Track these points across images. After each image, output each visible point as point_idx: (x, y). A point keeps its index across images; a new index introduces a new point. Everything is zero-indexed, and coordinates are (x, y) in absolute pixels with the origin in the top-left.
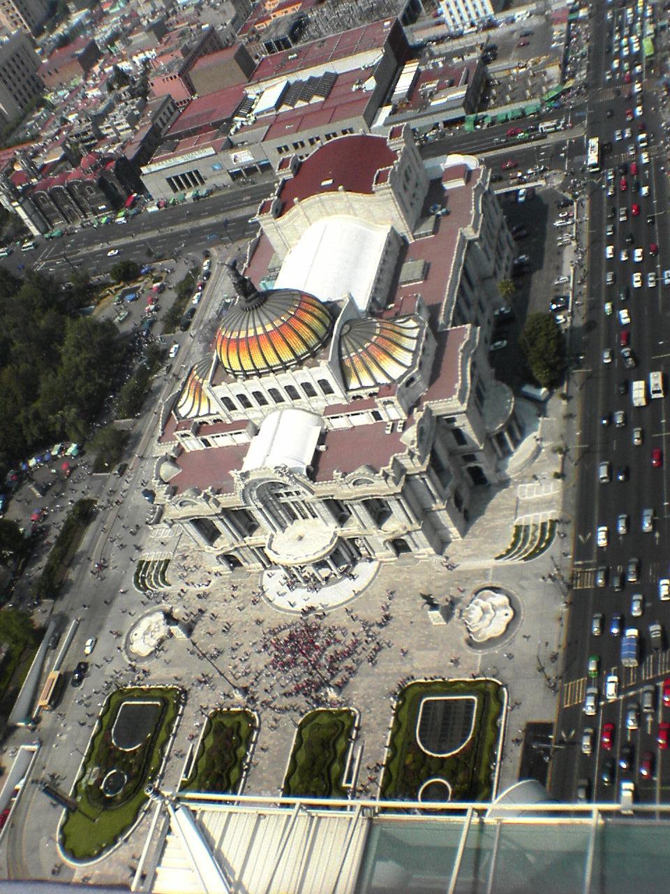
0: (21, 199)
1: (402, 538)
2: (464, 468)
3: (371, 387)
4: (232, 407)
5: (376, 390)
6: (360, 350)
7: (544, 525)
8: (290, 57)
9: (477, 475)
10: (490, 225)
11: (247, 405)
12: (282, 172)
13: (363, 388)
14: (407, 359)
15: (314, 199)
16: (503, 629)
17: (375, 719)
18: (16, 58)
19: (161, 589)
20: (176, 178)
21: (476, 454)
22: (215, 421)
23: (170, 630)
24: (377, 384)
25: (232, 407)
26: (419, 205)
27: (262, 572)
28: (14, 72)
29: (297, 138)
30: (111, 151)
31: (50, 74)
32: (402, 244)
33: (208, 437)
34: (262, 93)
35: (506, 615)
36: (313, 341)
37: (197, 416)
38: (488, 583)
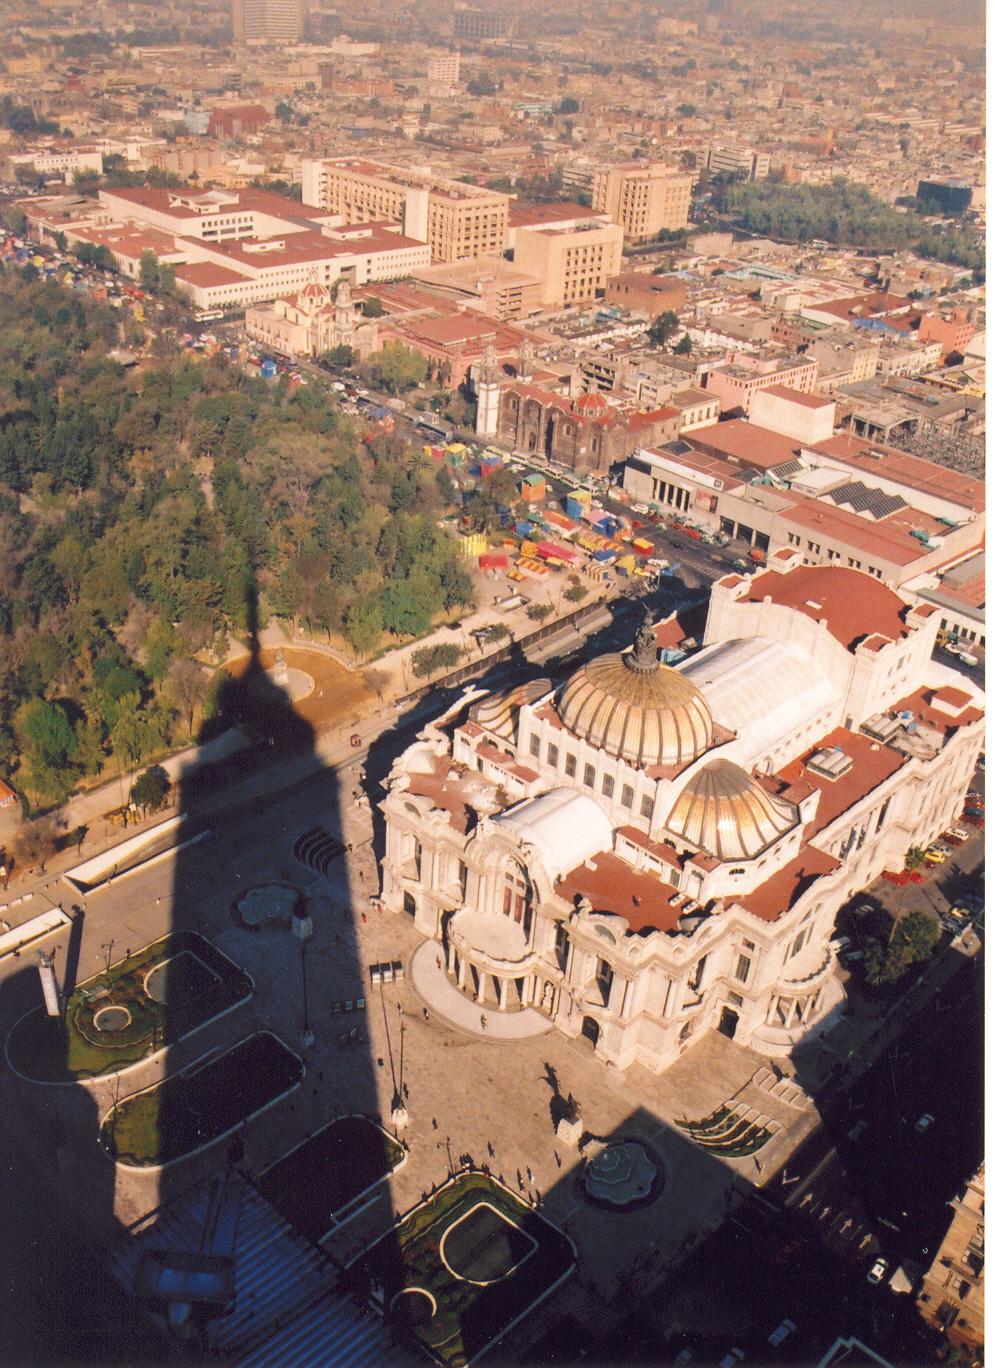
0: (494, 386)
1: (599, 1022)
2: (721, 1005)
3: (693, 844)
4: (535, 751)
5: (694, 850)
6: (712, 798)
7: (756, 1130)
8: (873, 453)
9: (729, 1023)
10: (950, 778)
11: (553, 762)
12: (777, 560)
13: (682, 836)
14: (754, 846)
15: (786, 611)
16: (623, 1202)
17: (418, 1180)
18: (597, 249)
19: (315, 872)
20: (663, 485)
21: (745, 1000)
22: (507, 751)
23: (291, 918)
24: (700, 846)
25: (535, 751)
26: (893, 700)
27: (428, 939)
28: (584, 261)
29: (818, 538)
30: (619, 409)
31: (618, 288)
32: (843, 726)
33: (487, 763)
34: (816, 467)
35: (641, 1189)
36: (670, 753)
37: (492, 731)
38: (649, 1140)
